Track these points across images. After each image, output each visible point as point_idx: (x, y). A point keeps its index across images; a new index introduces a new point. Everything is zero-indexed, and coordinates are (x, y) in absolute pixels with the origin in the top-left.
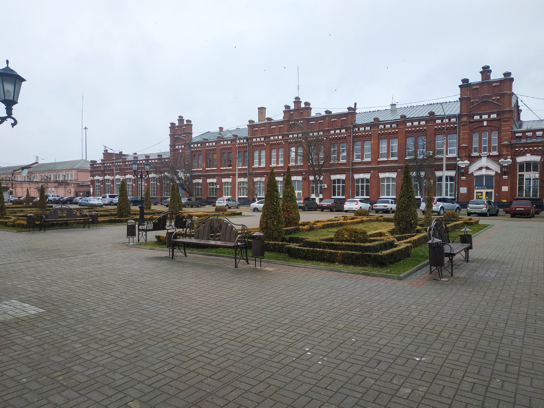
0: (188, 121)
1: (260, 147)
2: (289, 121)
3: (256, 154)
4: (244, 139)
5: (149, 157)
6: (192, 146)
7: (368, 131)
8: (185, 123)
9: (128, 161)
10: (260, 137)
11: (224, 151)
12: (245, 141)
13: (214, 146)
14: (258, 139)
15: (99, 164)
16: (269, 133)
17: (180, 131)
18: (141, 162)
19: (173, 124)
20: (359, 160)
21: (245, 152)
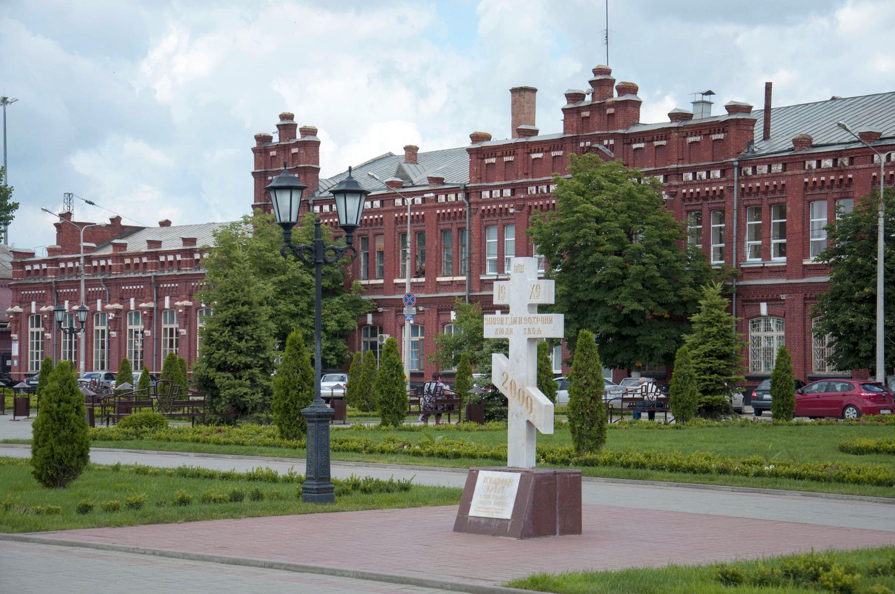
0: (306, 131)
1: (497, 216)
2: (576, 140)
3: (492, 240)
4: (455, 190)
5: (193, 241)
6: (317, 209)
7: (777, 176)
8: (299, 136)
9: (132, 256)
10: (501, 188)
11: (445, 225)
12: (461, 196)
13: (378, 211)
14: (496, 194)
15: (40, 262)
16: (526, 175)
17: (284, 157)
18: (171, 258)
19: (263, 140)
20: (757, 262)
21: (461, 230)
